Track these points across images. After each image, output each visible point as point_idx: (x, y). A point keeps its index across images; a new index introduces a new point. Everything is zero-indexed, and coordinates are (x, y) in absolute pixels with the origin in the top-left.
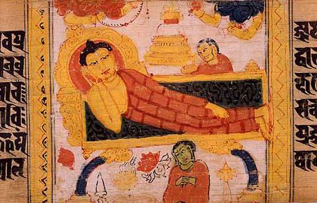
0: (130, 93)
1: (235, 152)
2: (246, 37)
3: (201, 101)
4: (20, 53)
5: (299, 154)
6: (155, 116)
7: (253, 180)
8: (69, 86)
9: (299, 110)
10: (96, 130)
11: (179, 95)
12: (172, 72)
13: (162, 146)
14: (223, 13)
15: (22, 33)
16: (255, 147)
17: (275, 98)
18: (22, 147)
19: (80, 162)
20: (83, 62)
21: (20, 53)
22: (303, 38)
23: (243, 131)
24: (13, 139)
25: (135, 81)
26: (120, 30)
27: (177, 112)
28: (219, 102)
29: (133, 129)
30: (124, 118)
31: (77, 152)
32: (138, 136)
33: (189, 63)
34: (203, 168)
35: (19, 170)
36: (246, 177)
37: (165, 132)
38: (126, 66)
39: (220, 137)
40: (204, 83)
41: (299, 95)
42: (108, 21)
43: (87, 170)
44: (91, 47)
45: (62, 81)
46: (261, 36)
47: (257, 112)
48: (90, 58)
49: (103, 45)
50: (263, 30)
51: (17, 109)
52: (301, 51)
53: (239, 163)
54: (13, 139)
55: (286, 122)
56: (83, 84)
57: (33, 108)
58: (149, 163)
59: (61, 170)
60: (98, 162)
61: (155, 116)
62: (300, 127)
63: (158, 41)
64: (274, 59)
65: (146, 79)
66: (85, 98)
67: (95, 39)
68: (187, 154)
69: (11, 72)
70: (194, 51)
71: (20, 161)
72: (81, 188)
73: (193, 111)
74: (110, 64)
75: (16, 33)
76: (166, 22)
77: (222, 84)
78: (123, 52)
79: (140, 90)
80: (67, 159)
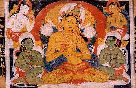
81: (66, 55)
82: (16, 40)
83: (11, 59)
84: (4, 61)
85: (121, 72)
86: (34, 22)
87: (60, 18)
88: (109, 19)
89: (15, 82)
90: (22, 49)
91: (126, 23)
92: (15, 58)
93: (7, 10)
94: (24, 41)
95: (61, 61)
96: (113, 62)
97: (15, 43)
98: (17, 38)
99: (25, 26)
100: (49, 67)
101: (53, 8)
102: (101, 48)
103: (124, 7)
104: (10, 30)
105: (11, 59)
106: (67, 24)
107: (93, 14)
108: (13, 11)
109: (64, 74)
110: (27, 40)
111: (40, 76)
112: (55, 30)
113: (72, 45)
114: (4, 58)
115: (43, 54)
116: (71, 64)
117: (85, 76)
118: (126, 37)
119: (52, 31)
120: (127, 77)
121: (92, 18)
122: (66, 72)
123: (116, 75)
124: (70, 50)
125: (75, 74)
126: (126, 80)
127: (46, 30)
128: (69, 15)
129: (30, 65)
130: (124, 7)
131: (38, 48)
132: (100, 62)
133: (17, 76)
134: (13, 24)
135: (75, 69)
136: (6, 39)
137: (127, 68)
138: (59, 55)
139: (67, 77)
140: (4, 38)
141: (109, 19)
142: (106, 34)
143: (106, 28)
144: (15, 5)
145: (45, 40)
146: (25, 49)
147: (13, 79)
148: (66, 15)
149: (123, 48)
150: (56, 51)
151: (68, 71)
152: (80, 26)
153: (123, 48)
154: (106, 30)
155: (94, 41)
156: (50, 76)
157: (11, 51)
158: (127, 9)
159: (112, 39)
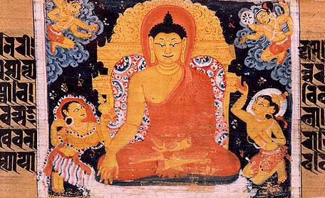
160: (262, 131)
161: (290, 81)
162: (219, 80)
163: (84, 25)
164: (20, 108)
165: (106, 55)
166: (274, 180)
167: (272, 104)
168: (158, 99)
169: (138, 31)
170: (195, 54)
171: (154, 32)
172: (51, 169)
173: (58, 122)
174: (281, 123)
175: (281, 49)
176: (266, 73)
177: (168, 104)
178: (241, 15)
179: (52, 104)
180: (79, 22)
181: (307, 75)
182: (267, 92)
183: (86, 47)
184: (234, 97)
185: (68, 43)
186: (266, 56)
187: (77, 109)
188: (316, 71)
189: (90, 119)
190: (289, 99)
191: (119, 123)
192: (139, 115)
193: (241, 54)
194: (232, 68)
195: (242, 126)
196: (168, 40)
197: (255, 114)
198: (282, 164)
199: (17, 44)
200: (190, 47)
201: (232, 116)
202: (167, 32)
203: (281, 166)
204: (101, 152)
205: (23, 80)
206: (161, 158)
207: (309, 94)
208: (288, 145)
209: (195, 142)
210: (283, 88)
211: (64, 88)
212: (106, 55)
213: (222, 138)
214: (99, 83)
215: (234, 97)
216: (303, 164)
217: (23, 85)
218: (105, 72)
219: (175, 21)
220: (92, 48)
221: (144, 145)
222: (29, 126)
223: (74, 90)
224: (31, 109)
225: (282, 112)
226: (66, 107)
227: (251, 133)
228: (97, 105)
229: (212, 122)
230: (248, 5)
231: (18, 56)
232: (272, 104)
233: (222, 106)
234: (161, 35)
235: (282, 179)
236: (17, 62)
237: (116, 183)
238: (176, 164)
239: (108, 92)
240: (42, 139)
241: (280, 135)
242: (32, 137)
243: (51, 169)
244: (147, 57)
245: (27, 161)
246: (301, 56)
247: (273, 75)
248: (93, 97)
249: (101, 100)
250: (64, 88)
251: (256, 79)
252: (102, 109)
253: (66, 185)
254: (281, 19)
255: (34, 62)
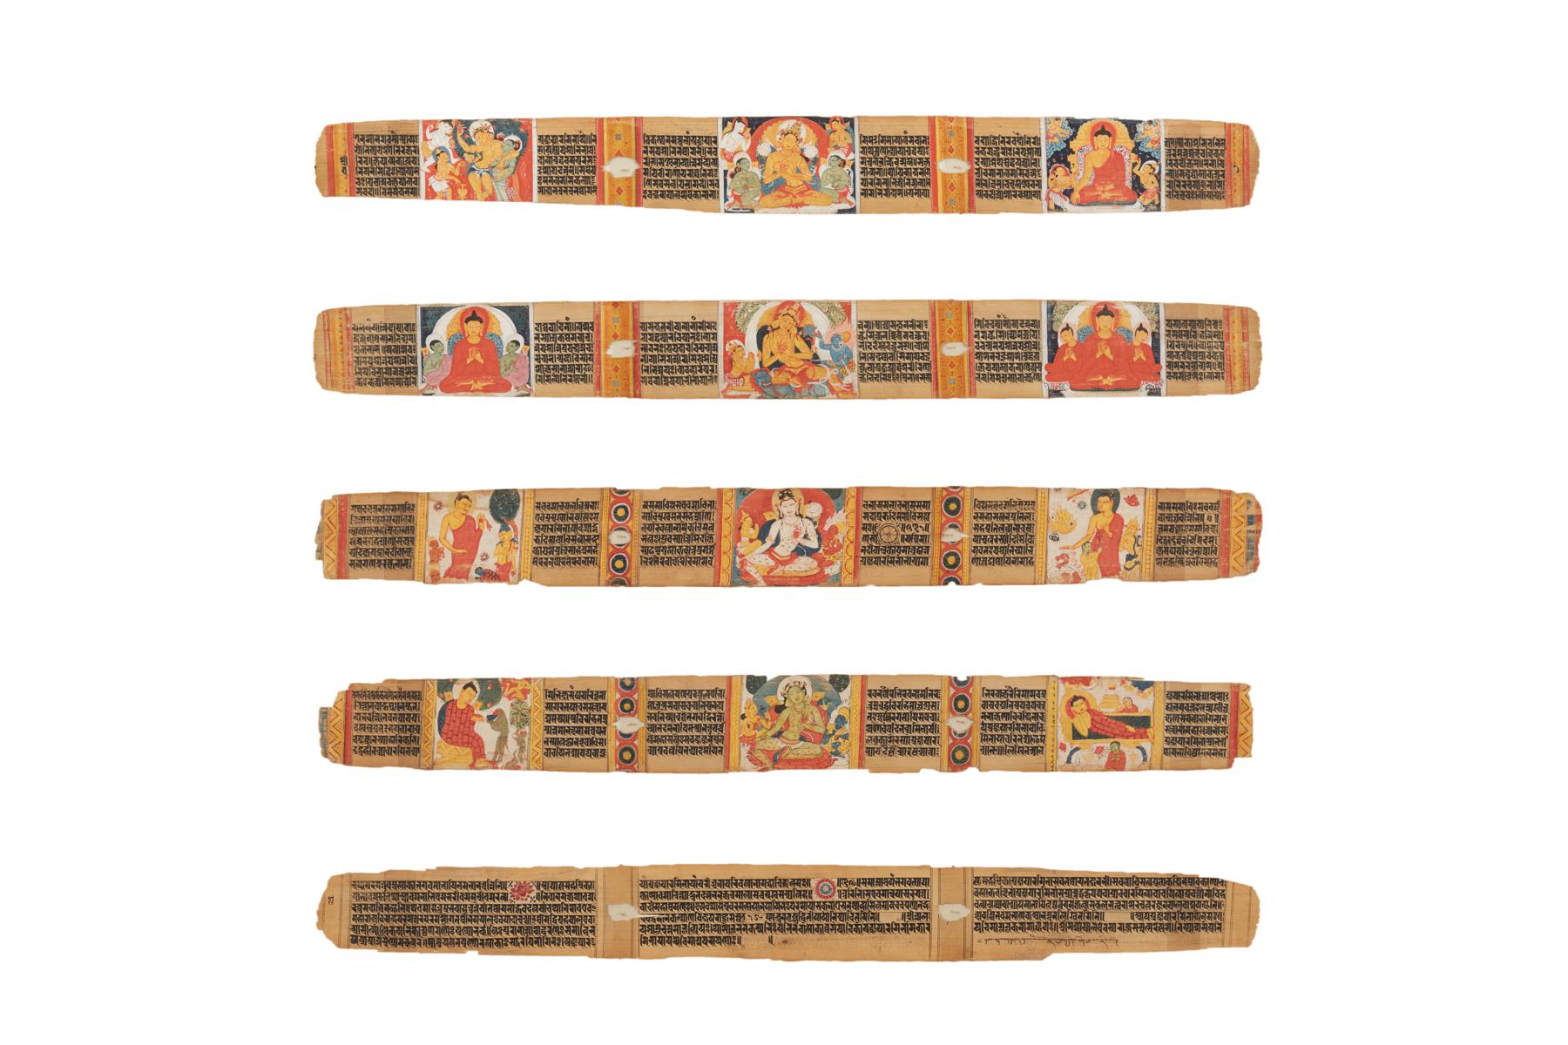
0: (1092, 720)
1: (1138, 747)
2: (1145, 697)
3: (1123, 725)
4: (1044, 699)
5: (1165, 749)
6: (1103, 730)
7: (1145, 760)
8: (1065, 715)
9: (1166, 730)
10: (1076, 735)
11: (1114, 721)
12: (1110, 711)
13: (1105, 743)
14: (1135, 686)
15: (1045, 691)
16: (1146, 744)
17: (1156, 725)
18: (1043, 741)
19: (1069, 749)
20: (1072, 705)
21: (1044, 699)
22: (1170, 699)
23: (1142, 738)
24: (1039, 737)
25: (1095, 714)
26: (1090, 692)
27: (1113, 729)
28: (1132, 725)
29: (1093, 735)
30: (1089, 730)
31: (1068, 744)
32: (1095, 738)
33: (1119, 707)
34: (1122, 754)
35: (1041, 752)
36: (1142, 759)
37: (1108, 737)
38: (1091, 707)
39: (1131, 741)
40: (1125, 717)
41: (1167, 724)
42: (1084, 687)
43: (1072, 753)
44: (1076, 698)
45: (1062, 713)
46: (1151, 697)
47: (1148, 730)
48: (1075, 703)
49: (1081, 697)
50: (1152, 694)
51: (1042, 724)
52: (1168, 704)
53: (1139, 752)
54: (1039, 737)
55: (1161, 735)
56: (1071, 714)
57: (1048, 724)
58: (1099, 750)
59: (1061, 752)
60: (1077, 749)
61: (1103, 730)
62: (1167, 738)
63: (1106, 697)
64: (1157, 708)
65: (1100, 714)
66: (1072, 721)
67: (1078, 695)
68: (1116, 747)
69: (1039, 708)
70: (1122, 702)
71: (1042, 747)
72: (1069, 760)
73: (1120, 729)
74: (1084, 707)
75: (1043, 691)
76: (1110, 689)
77: (1133, 717)
78: (1090, 701)
79: (1097, 718)
80: (1063, 747)
81: (785, 176)
82: (730, 160)
83: (725, 181)
84: (718, 184)
85: (845, 194)
86: (750, 141)
87: (779, 136)
88: (833, 136)
89: (730, 205)
90: (738, 170)
91: (850, 141)
92: (729, 180)
93: (720, 127)
94: (739, 161)
95: (780, 185)
96: (836, 184)
97: (730, 163)
98: (732, 158)
99: (740, 146)
100: (766, 189)
101: (771, 125)
102: (823, 168)
103: (849, 123)
104: (723, 149)
105: (725, 181)
106: (786, 143)
107: (814, 132)
108: (727, 129)
109: (784, 197)
110: (742, 161)
111: (757, 199)
112: (773, 150)
113: (791, 166)
114: (718, 180)
115: (760, 176)
116: (790, 186)
117: (807, 200)
118: (851, 156)
119: (770, 150)
120: (851, 199)
121: (813, 136)
122: (784, 195)
123: (840, 197)
124: (789, 171)
125: (795, 197)
126: (851, 203)
127: (763, 150)
128: (788, 133)
129: (746, 187)
130: (849, 123)
131: (755, 169)
132: (822, 184)
133: (731, 200)
134: (727, 143)
135: (795, 192)
136: (719, 160)
137: (851, 190)
138: (777, 176)
139: (787, 201)
140: (717, 159)
141: (833, 136)
142: (828, 153)
143: (829, 146)
144: (729, 123)
145: (762, 161)
146: (740, 170)
147: (727, 203)
148: (785, 133)
149: (848, 167)
150: (775, 172)
151: (788, 193)
152: (800, 145)
153: (848, 167)
154: (829, 149)
155: (816, 162)
156: (768, 199)
157: (726, 172)
158: (852, 125)
159: (836, 159)
160: (1147, 181)
161: (1160, 157)
162: (1127, 157)
163: (1064, 131)
164: (1034, 170)
165: (1073, 145)
166: (1153, 203)
167: (1152, 168)
168: (1098, 165)
169: (1089, 134)
170: (1116, 144)
171: (1096, 135)
172: (1048, 199)
173: (1051, 176)
174: (1156, 176)
175: (1156, 142)
176: (1149, 153)
177: (1104, 168)
178: (1137, 126)
179: (1049, 168)
180: (1061, 130)
181: (1168, 154)
182: (1150, 162)
183: (1064, 142)
184: (1134, 165)
185: (1056, 140)
186: (1149, 145)
187: (1060, 171)
188: (1172, 152)
189: (1067, 174)
190: (1160, 165)
191: (1080, 177)
192: (1091, 174)
193: (1138, 145)
194: (1133, 151)
195: (1138, 178)
196: (1103, 138)
197: (1144, 172)
198: (1157, 196)
199: (1032, 140)
200: (1114, 141)
201: (1133, 174)
202: (1103, 134)
203: (1156, 197)
204: (1072, 190)
205: (1035, 157)
206: (1100, 193)
207: (1169, 163)
208: (1160, 187)
209: (1116, 186)
210: (1157, 160)
211: (1054, 160)
212: (1073, 145)
213: (1128, 184)
214: (1070, 158)
215: (1134, 165)
216: (1167, 196)
217: (1035, 159)
218: (1073, 153)
219: (1106, 129)
220: (1067, 142)
221: (1092, 188)
222: (1038, 178)
223: (1059, 161)
224: (1039, 170)
225: (1157, 172)
226: (1055, 169)
227: (1142, 181)
228: (1070, 168)
229: (1124, 176)
230: (1140, 122)
231: (1033, 146)
232: (1152, 168)
233: (1128, 169)
234: (1100, 136)
235: (1157, 203)
236: (1032, 148)
237: (1079, 205)
238: (1107, 196)
239: (1075, 162)
240: (1044, 184)
241: (1156, 182)
242: (1039, 184)
243: (1048, 199)
244: (1093, 146)
245: (1037, 195)
246: (1166, 145)
247: (1152, 154)
248: (1068, 165)
249: (1072, 166)
250: (1054, 160)
251: (1144, 157)
252: (1073, 170)
253: (1056, 206)
254: (1157, 128)
255: (1040, 148)
